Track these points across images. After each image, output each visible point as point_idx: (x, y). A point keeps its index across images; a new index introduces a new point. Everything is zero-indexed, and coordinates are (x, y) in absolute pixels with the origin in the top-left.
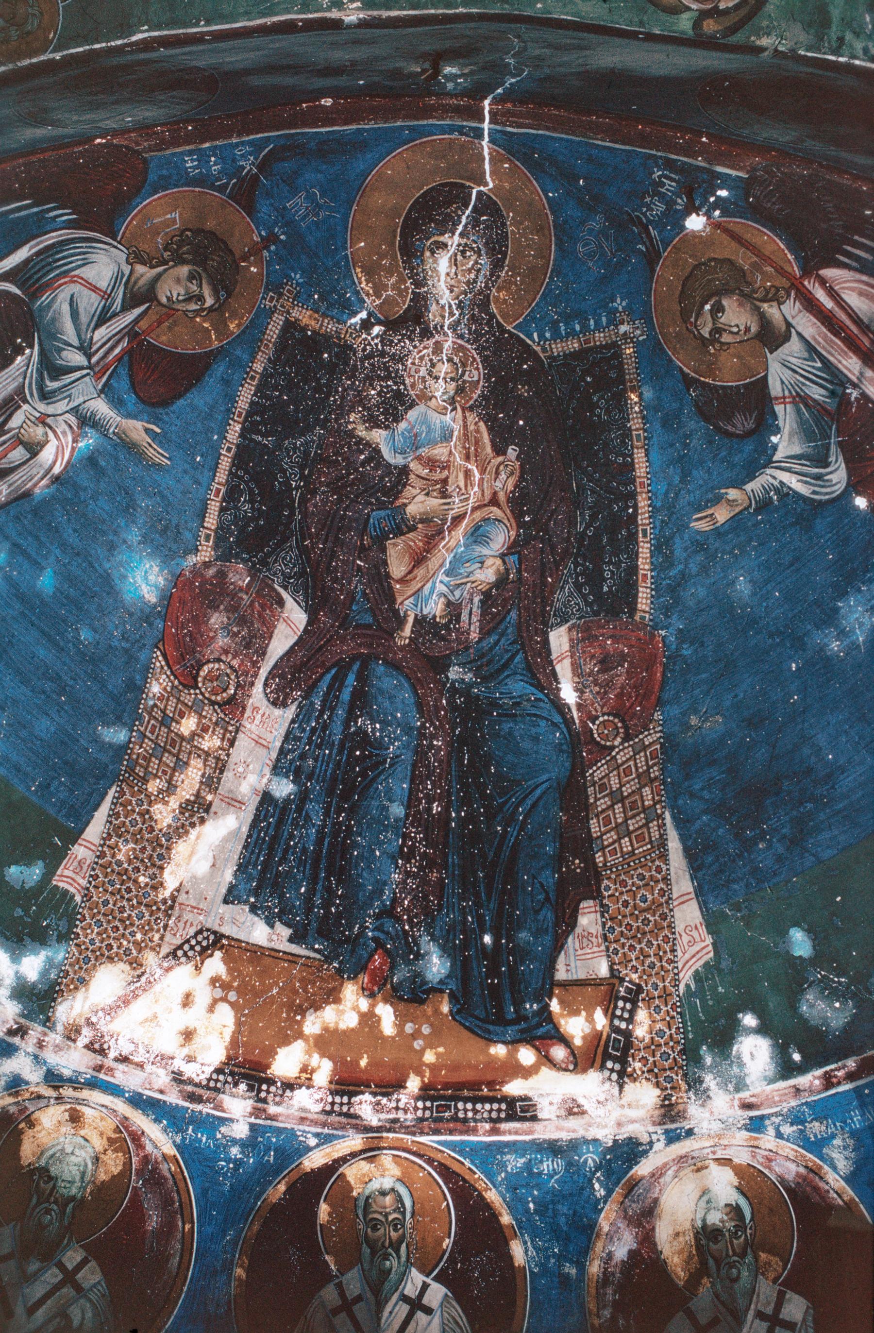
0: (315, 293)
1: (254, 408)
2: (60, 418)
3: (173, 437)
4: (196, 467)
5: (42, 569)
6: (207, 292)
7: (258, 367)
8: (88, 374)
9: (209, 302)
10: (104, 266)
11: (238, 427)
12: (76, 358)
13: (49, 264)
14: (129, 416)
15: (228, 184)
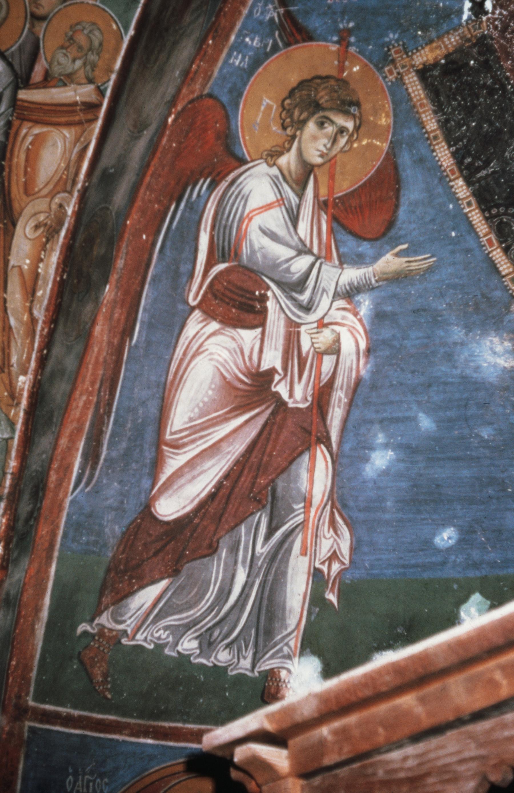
0: (416, 31)
1: (459, 157)
2: (332, 312)
3: (421, 239)
4: (456, 241)
5: (414, 419)
6: (341, 121)
7: (432, 125)
8: (321, 264)
9: (350, 125)
10: (258, 186)
11: (460, 182)
12: (302, 264)
13: (225, 227)
14: (376, 259)
15: (275, 40)
